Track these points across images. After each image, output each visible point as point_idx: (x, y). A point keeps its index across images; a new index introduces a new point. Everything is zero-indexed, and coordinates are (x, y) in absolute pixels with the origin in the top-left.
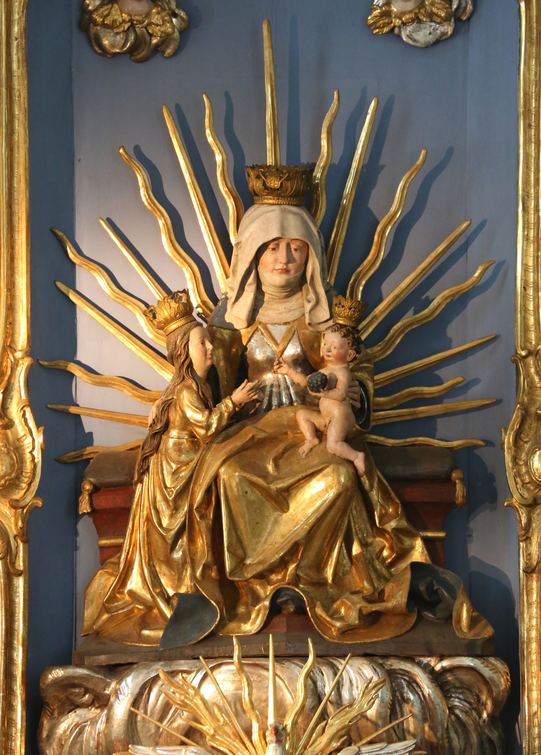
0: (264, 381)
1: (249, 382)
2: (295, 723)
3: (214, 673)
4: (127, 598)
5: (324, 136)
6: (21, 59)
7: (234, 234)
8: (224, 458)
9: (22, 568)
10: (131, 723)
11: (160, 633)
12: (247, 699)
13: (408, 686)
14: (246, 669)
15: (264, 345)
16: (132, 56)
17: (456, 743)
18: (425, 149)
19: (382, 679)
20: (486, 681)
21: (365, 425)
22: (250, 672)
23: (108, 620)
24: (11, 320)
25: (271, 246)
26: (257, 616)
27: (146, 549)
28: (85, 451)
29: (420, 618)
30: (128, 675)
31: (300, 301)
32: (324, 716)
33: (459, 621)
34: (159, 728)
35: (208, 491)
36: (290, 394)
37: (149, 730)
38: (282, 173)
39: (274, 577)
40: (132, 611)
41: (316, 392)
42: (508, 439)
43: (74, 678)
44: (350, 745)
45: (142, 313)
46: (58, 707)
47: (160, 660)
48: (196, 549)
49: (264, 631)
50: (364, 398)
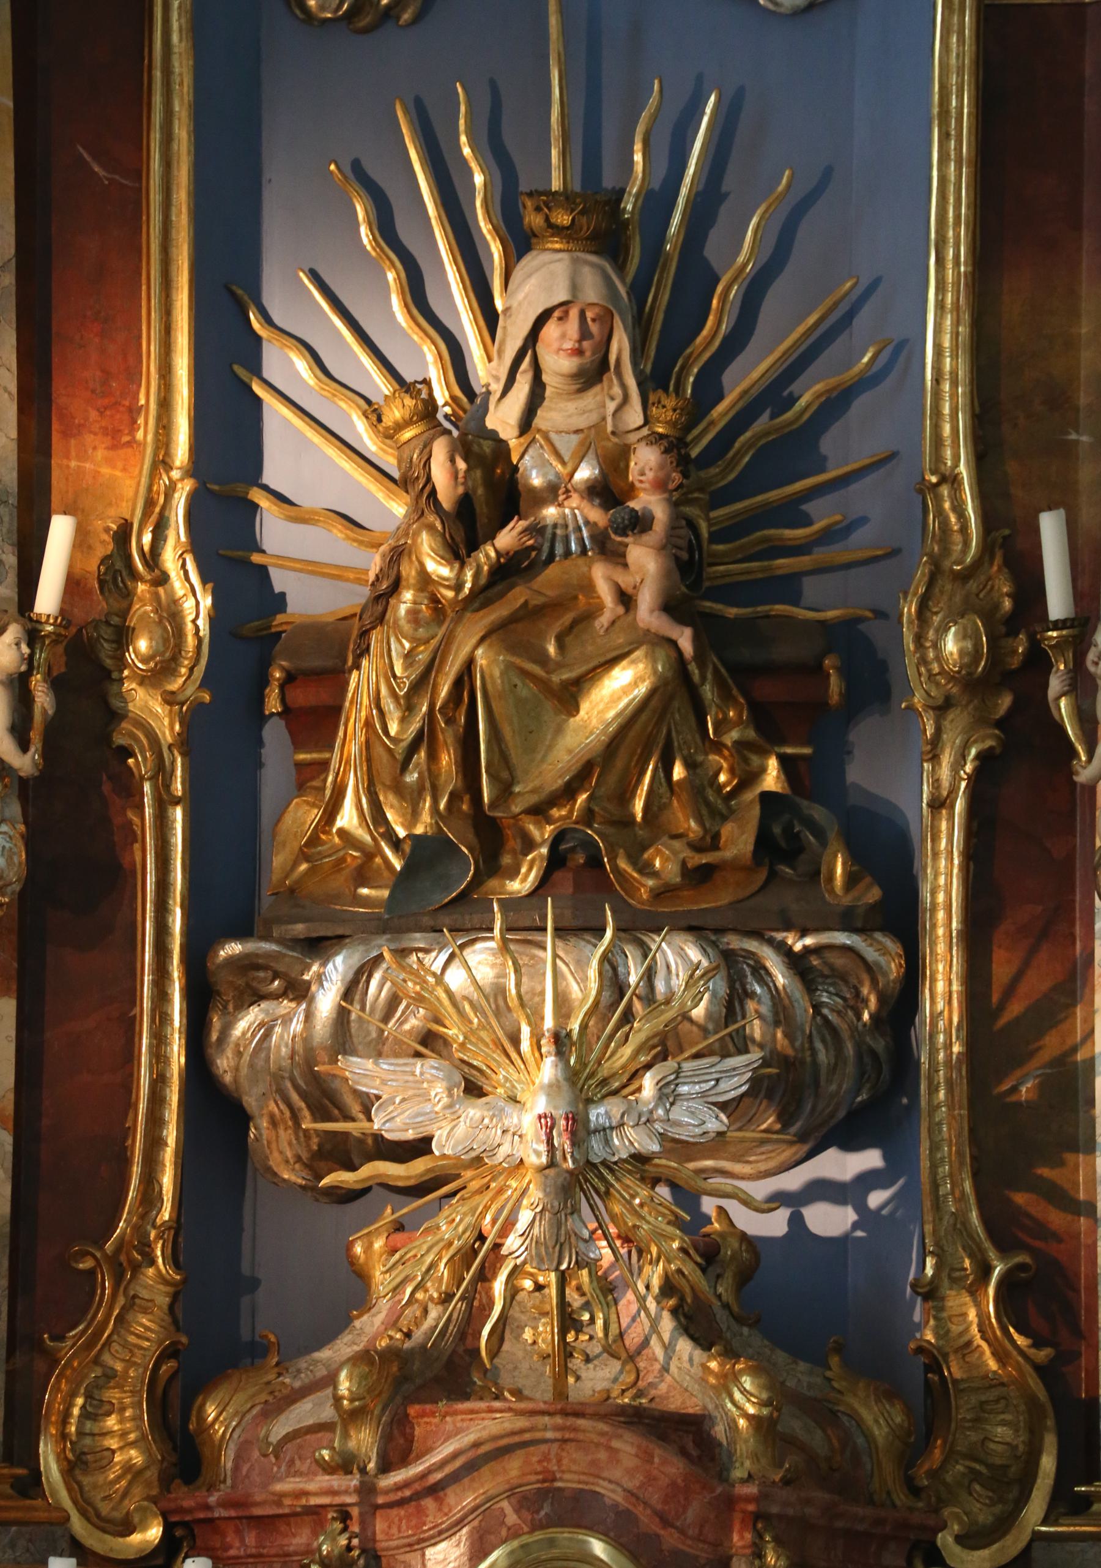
0: (544, 518)
1: (520, 519)
2: (584, 1027)
3: (465, 953)
4: (337, 840)
5: (638, 147)
6: (184, 26)
7: (501, 295)
8: (481, 634)
9: (180, 794)
10: (342, 1024)
11: (385, 893)
12: (514, 991)
13: (753, 974)
14: (512, 947)
15: (543, 464)
16: (350, 23)
17: (822, 1056)
18: (791, 168)
19: (714, 964)
20: (869, 968)
21: (694, 586)
22: (517, 952)
23: (308, 870)
24: (165, 421)
25: (556, 314)
26: (530, 870)
27: (365, 768)
28: (274, 620)
29: (773, 875)
30: (337, 954)
31: (598, 398)
32: (628, 1017)
33: (831, 877)
34: (383, 1031)
35: (458, 684)
36: (583, 539)
37: (368, 1033)
38: (574, 203)
39: (555, 813)
40: (343, 860)
41: (621, 536)
42: (909, 609)
43: (257, 955)
44: (665, 1059)
45: (360, 413)
46: (233, 997)
47: (384, 932)
48: (439, 769)
49: (540, 891)
50: (694, 546)
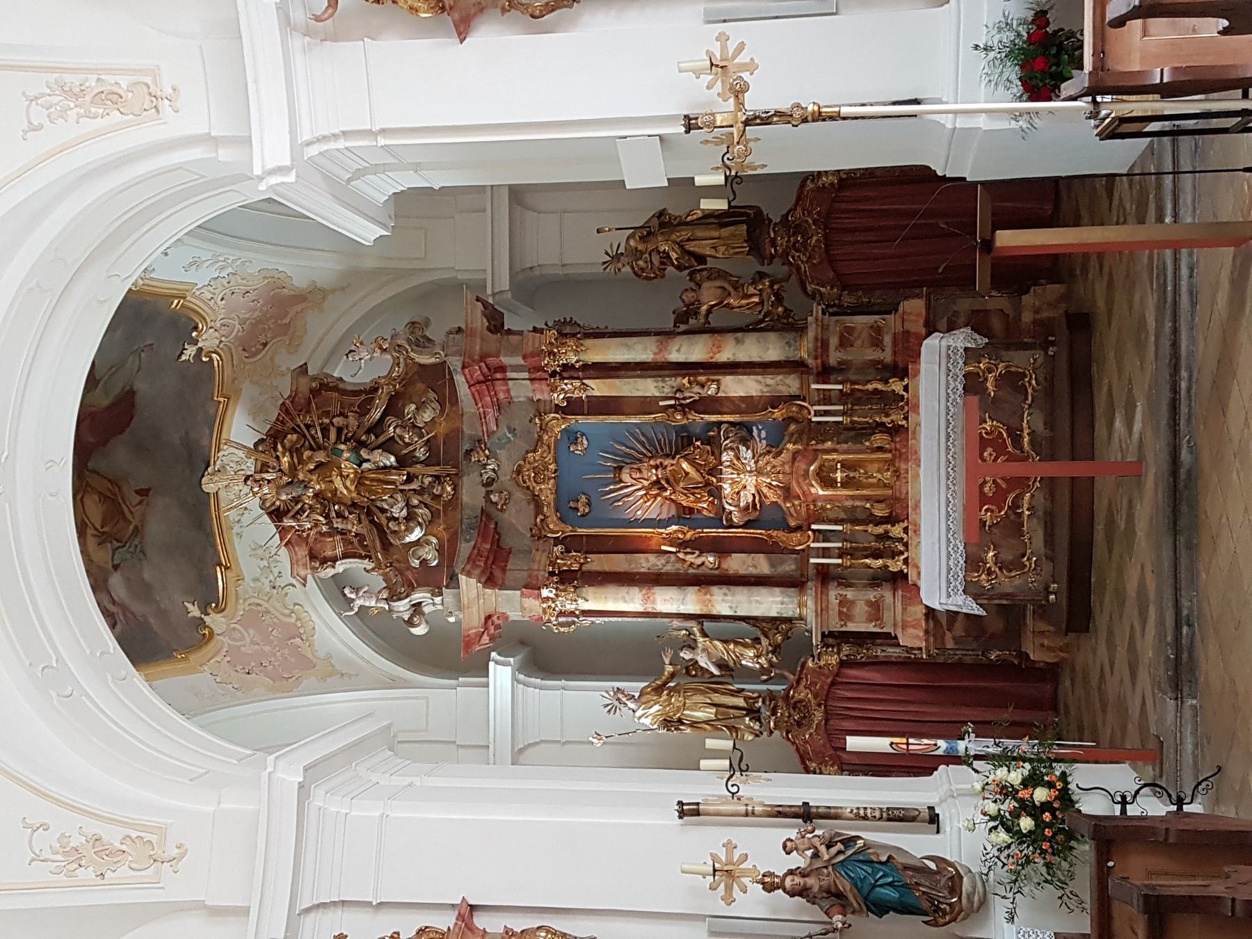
42: (673, 424)
